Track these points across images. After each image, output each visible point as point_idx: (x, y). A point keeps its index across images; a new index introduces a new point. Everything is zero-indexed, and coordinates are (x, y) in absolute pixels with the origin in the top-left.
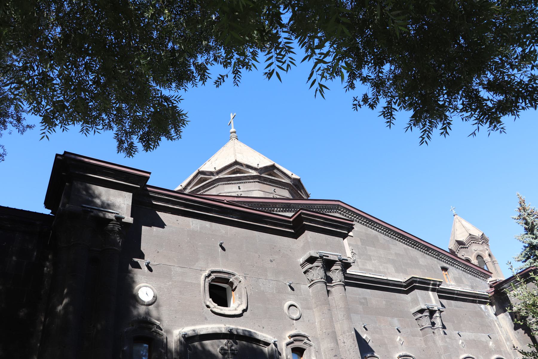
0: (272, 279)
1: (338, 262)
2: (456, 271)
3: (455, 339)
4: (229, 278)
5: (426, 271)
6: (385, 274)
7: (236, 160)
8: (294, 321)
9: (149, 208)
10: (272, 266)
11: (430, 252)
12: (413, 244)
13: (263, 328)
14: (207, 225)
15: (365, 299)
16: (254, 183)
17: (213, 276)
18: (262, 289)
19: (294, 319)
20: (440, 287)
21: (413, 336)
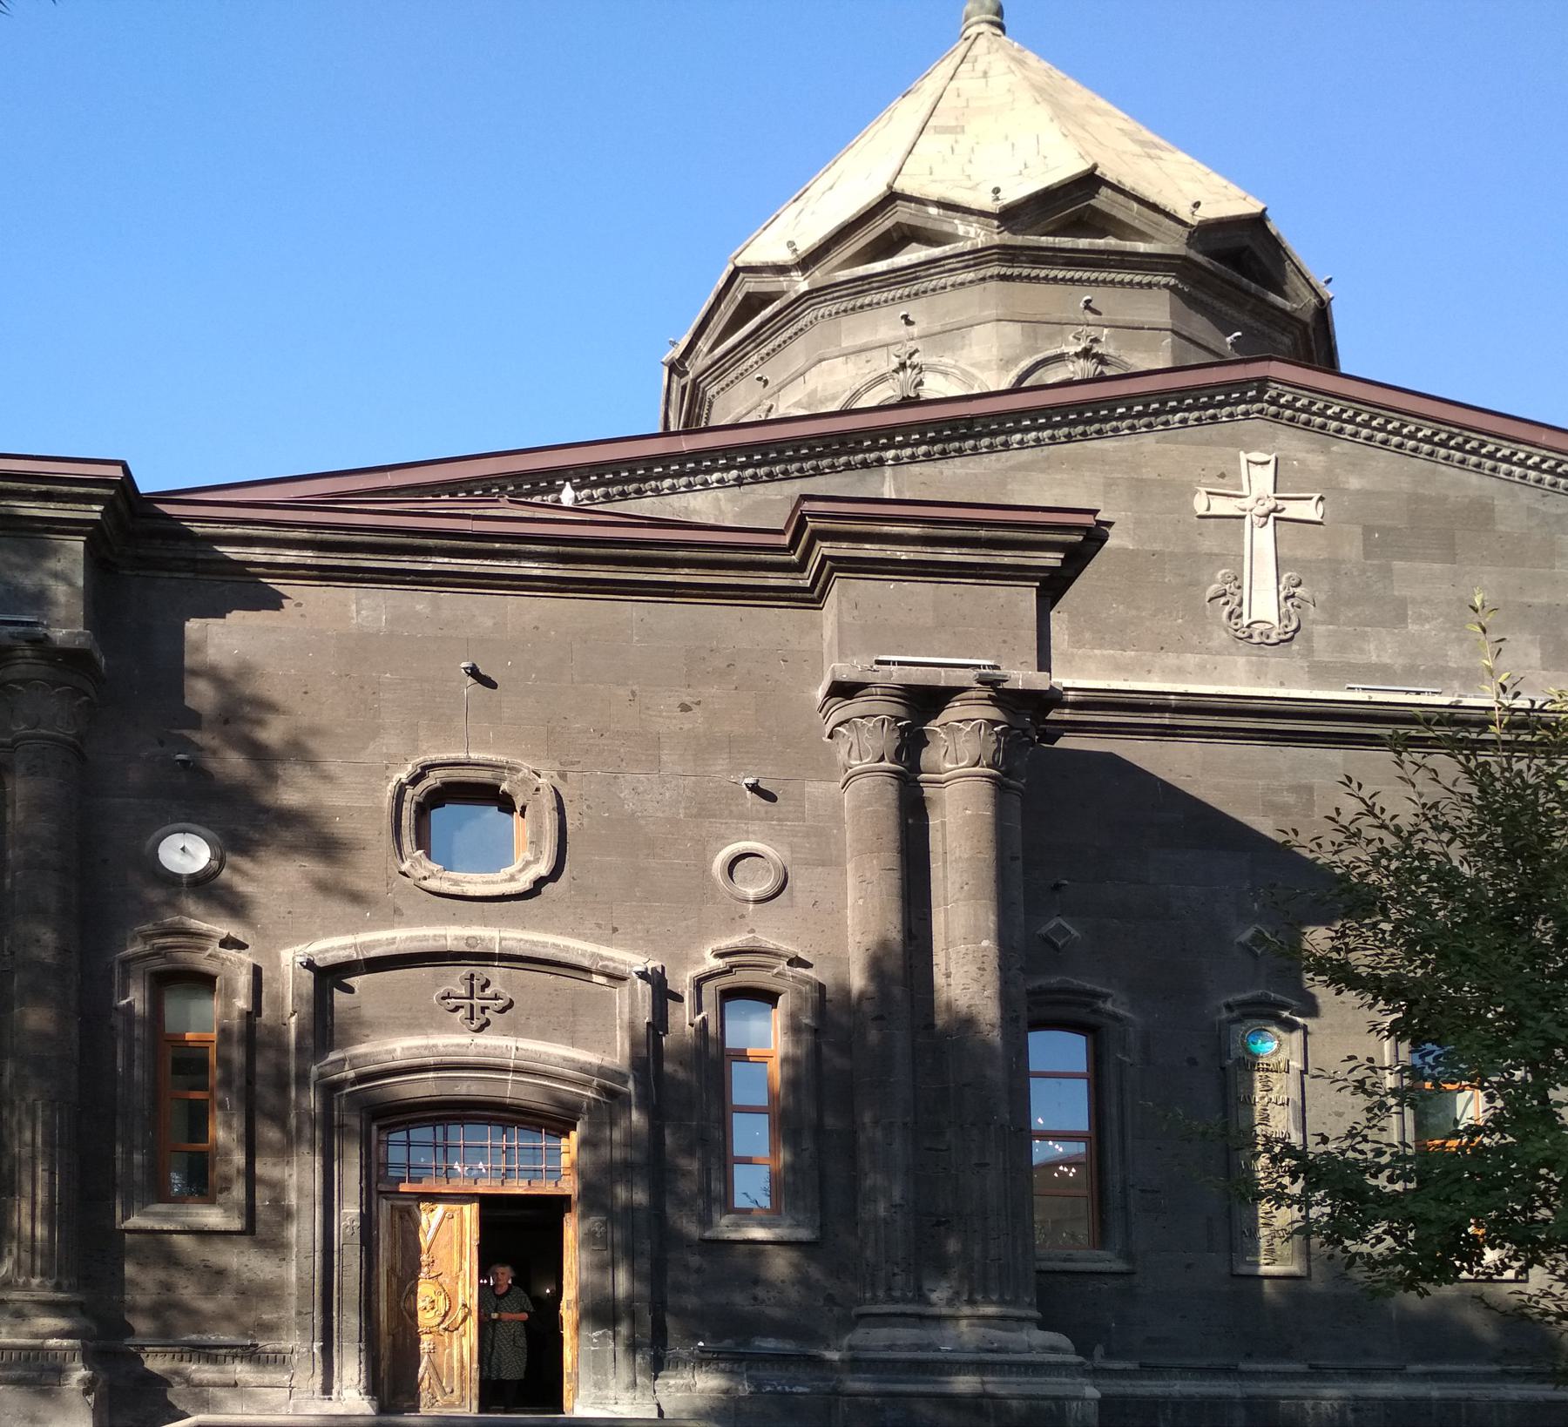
0: (679, 770)
4: (497, 782)
9: (182, 575)
18: (630, 806)
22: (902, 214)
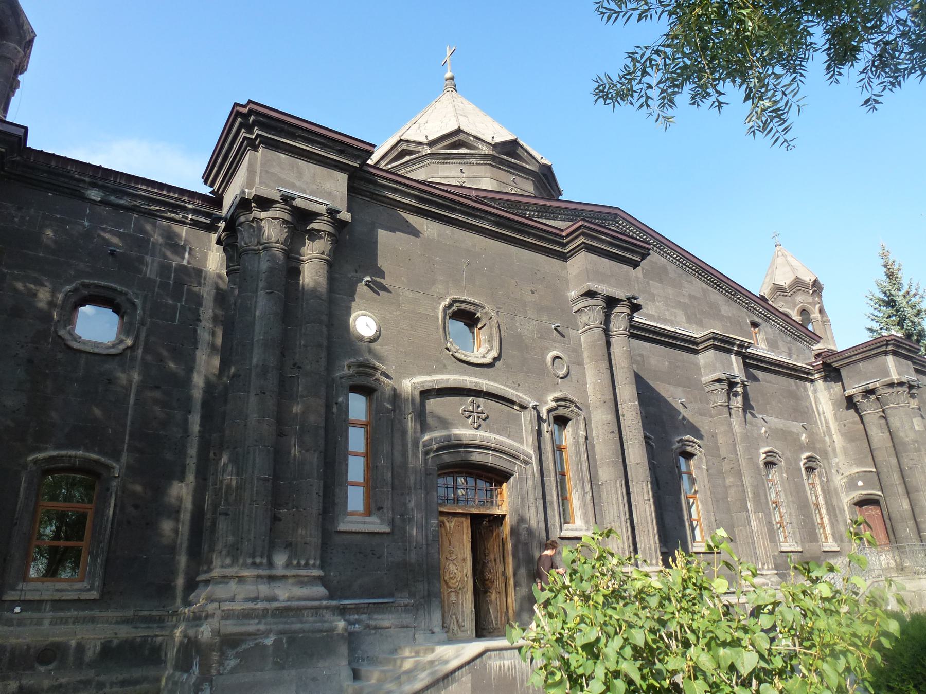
1: (624, 303)
2: (770, 330)
5: (729, 325)
7: (459, 127)
8: (560, 380)
9: (367, 199)
10: (534, 300)
11: (738, 298)
12: (715, 284)
13: (519, 385)
15: (641, 356)
17: (456, 307)
18: (519, 330)
20: (748, 350)
22: (461, 137)
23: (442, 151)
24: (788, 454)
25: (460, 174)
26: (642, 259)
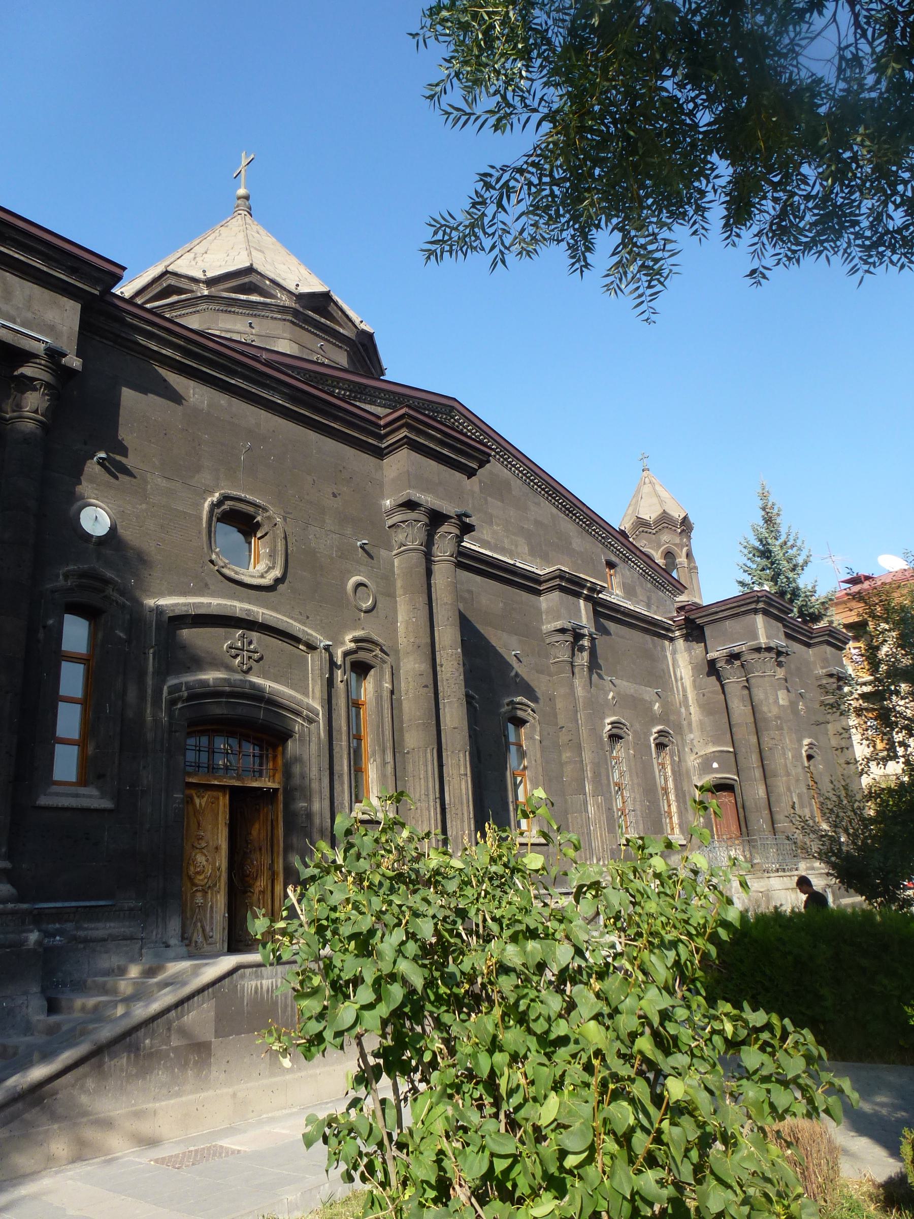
0: (332, 529)
1: (453, 520)
3: (603, 689)
5: (580, 562)
6: (511, 555)
7: (252, 265)
10: (335, 506)
11: (594, 530)
12: (568, 509)
13: (308, 617)
14: (222, 402)
15: (470, 592)
16: (282, 323)
18: (313, 545)
19: (361, 611)
20: (600, 595)
21: (537, 672)
22: (253, 278)
23: (225, 294)
24: (637, 726)
25: (248, 329)
26: (480, 467)
